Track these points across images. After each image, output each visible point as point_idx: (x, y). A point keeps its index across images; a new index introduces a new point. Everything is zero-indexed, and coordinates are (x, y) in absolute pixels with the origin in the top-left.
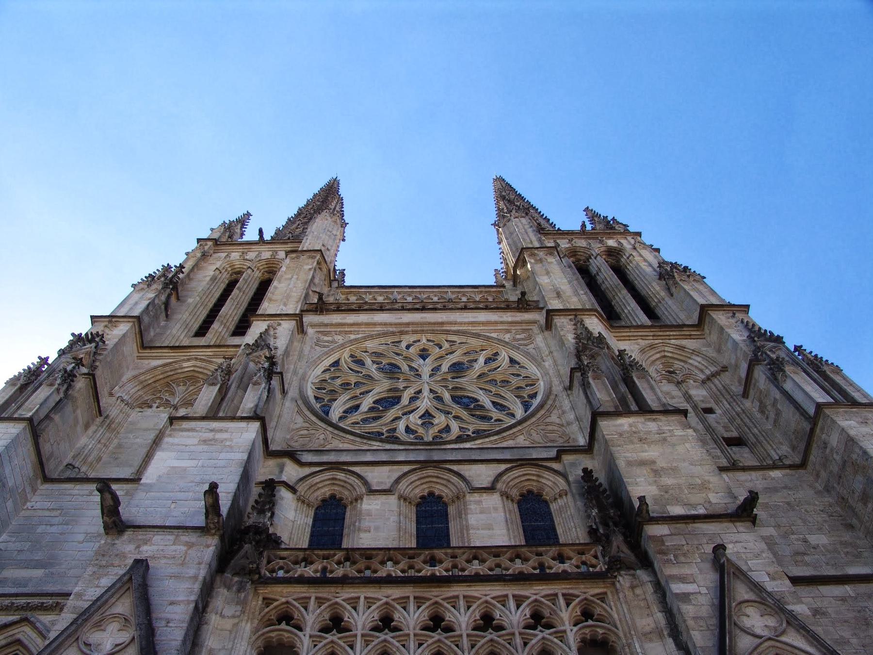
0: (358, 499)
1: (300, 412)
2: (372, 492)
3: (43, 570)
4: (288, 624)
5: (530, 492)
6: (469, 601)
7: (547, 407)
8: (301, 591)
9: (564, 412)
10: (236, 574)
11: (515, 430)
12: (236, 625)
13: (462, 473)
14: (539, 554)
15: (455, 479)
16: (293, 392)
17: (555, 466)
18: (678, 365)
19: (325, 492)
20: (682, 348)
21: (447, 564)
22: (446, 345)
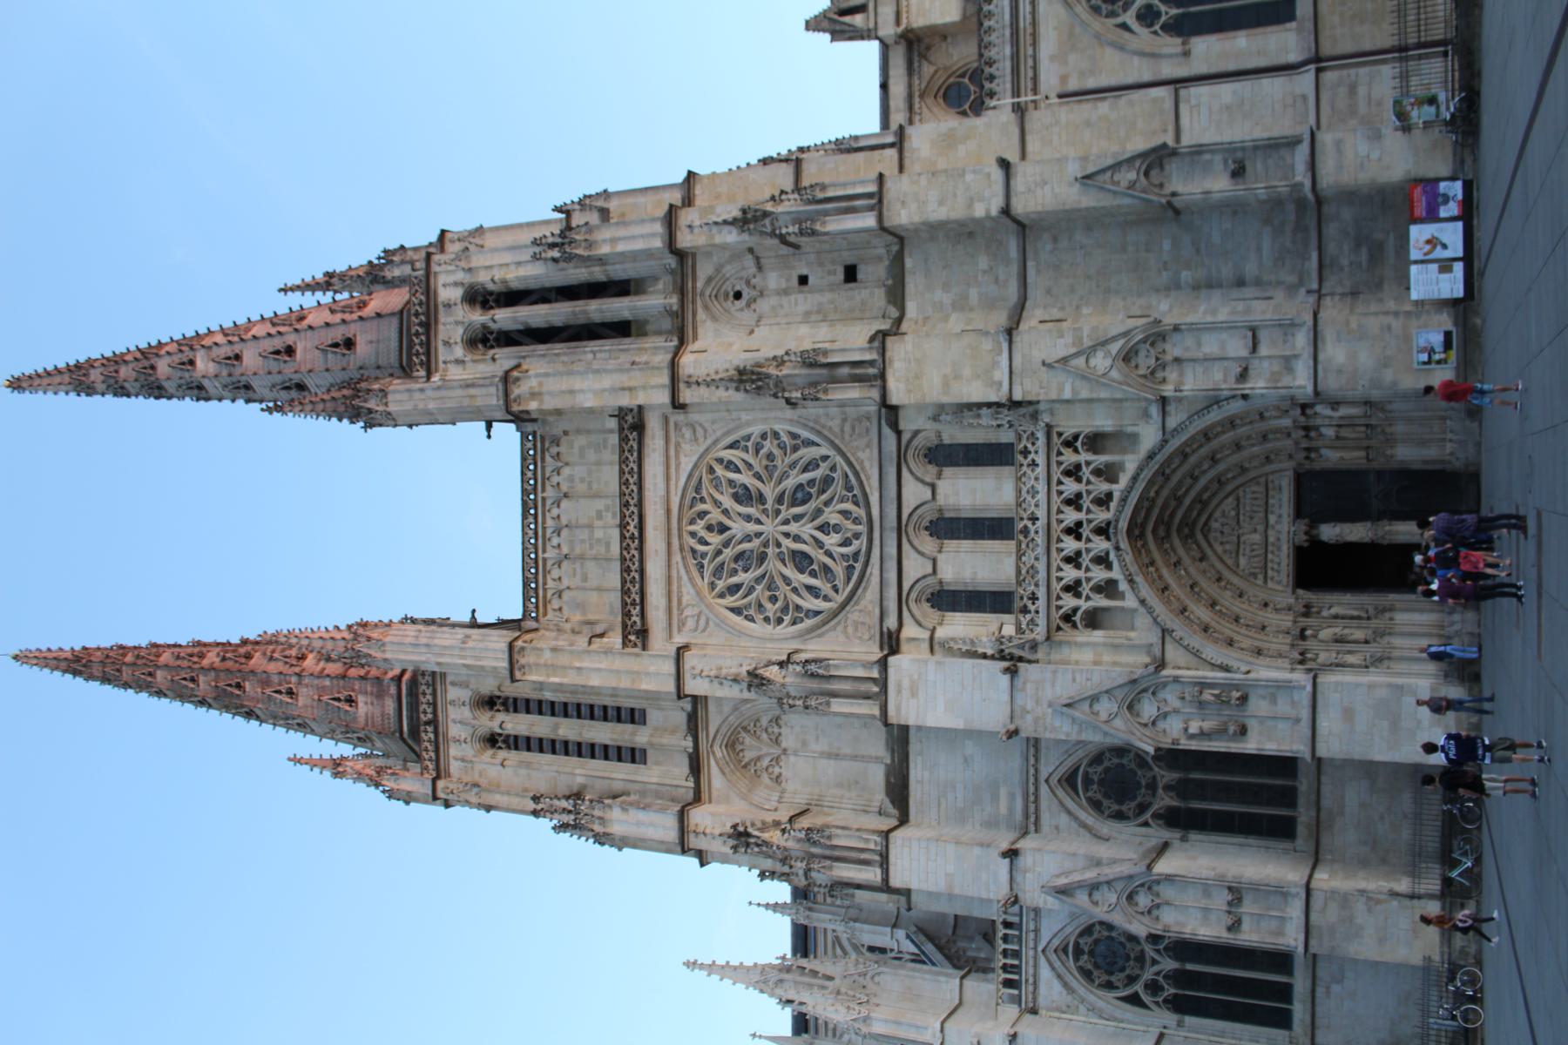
0: (941, 582)
1: (820, 636)
2: (935, 571)
5: (925, 456)
6: (1060, 511)
7: (818, 428)
9: (827, 415)
11: (852, 459)
14: (1022, 465)
15: (919, 512)
16: (795, 645)
17: (906, 437)
18: (728, 287)
19: (926, 606)
20: (709, 280)
21: (1029, 524)
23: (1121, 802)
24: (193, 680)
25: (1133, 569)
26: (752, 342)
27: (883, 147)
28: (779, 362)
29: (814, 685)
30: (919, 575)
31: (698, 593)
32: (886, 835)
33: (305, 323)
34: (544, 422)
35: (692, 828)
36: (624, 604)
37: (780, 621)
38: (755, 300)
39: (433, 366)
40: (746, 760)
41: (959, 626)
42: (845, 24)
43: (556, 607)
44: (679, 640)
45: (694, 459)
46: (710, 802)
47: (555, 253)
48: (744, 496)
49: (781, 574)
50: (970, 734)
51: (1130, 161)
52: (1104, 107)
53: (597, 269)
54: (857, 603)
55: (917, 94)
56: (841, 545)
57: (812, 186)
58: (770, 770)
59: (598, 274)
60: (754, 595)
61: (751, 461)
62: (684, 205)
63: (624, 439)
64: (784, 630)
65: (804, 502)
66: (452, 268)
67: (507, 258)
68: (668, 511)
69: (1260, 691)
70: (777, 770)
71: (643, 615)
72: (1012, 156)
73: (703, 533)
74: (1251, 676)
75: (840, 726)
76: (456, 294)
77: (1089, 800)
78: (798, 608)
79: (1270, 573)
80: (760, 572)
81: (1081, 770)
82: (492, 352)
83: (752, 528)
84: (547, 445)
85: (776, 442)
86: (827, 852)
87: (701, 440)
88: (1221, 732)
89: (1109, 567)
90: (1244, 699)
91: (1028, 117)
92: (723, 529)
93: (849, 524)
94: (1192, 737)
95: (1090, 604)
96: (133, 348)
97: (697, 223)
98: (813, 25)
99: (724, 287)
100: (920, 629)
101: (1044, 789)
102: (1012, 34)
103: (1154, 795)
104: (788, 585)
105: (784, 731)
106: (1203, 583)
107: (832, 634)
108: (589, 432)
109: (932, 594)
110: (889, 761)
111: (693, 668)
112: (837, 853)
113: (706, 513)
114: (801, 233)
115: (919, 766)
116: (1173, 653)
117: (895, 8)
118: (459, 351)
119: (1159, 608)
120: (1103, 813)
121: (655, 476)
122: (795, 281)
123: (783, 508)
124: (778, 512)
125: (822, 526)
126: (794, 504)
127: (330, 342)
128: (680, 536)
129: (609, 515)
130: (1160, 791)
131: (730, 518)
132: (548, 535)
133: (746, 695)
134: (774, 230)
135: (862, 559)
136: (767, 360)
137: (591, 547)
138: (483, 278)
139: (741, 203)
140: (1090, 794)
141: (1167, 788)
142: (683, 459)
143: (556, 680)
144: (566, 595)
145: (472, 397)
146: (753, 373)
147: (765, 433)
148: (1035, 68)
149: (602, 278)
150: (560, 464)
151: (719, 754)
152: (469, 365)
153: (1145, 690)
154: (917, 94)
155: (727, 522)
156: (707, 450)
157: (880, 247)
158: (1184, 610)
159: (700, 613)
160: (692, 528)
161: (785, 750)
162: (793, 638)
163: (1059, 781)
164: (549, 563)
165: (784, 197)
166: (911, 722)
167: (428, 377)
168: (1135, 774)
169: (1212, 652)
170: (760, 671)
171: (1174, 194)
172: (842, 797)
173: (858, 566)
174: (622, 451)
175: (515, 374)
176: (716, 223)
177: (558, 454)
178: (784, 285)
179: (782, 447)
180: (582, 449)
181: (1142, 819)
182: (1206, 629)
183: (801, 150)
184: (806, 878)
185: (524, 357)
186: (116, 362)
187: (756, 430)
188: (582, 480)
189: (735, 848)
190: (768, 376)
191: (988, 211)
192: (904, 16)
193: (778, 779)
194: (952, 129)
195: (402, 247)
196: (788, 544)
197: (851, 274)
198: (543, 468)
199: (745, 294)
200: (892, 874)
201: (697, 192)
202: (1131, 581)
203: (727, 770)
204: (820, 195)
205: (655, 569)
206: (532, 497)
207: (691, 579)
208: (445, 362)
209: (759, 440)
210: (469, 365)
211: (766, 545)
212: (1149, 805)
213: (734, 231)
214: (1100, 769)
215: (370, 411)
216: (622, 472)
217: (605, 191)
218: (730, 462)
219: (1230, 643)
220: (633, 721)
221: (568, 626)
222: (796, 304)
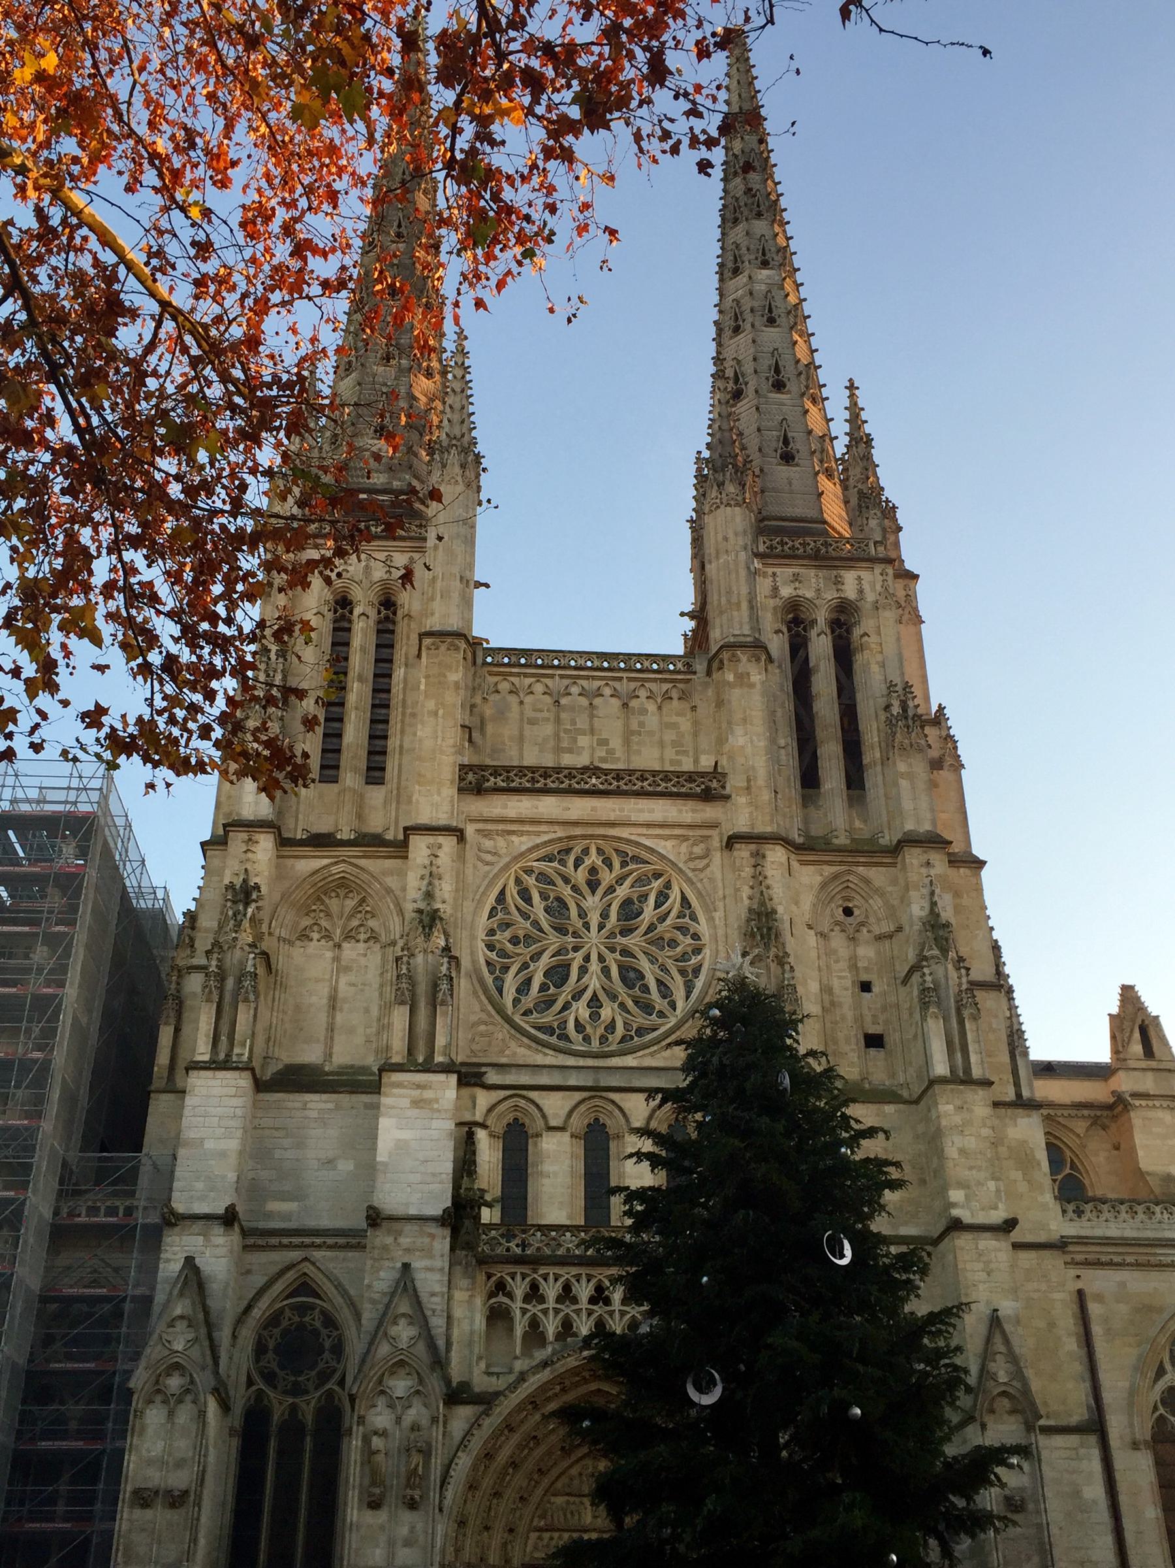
0: (538, 1135)
1: (475, 993)
3: (296, 1204)
4: (504, 1295)
8: (511, 1268)
10: (463, 1249)
12: (471, 1296)
13: (622, 1104)
15: (617, 1112)
16: (465, 963)
18: (855, 903)
19: (510, 1118)
20: (867, 881)
22: (616, 864)
23: (276, 1351)
24: (399, 235)
25: (560, 1367)
26: (800, 928)
27: (1017, 1084)
28: (781, 960)
29: (422, 988)
30: (545, 1109)
31: (522, 855)
32: (248, 1068)
33: (808, 404)
34: (706, 685)
35: (257, 837)
36: (508, 769)
37: (490, 947)
38: (843, 931)
39: (770, 561)
40: (327, 901)
41: (489, 1154)
42: (1132, 1031)
43: (500, 687)
44: (470, 830)
45: (672, 857)
46: (278, 857)
47: (896, 709)
48: (630, 910)
49: (544, 951)
50: (369, 1169)
51: (1018, 1374)
52: (1071, 1344)
53: (878, 755)
54: (512, 1037)
55: (1052, 1112)
56: (576, 1020)
57: (976, 1004)
58: (316, 928)
59: (871, 754)
60: (520, 919)
61: (668, 922)
62: (949, 854)
63: (691, 777)
64: (482, 953)
65: (623, 979)
66: (878, 588)
67: (890, 649)
68: (612, 824)
69: (419, 1527)
70: (315, 936)
71: (497, 790)
72: (1016, 1235)
73: (588, 862)
74: (438, 1516)
75: (367, 1010)
76: (850, 592)
77: (281, 1311)
78: (506, 969)
79: (546, 1535)
80: (545, 925)
81: (318, 1301)
82: (785, 630)
83: (594, 919)
84: (680, 686)
85: (689, 950)
86: (228, 997)
87: (692, 865)
88: (375, 1477)
89: (559, 1337)
90: (412, 1505)
91: (1055, 1253)
92: (593, 885)
93: (601, 1030)
94: (366, 1440)
95: (518, 1313)
96: (780, 189)
97: (933, 872)
98: (1128, 994)
99: (858, 897)
100: (485, 1111)
101: (296, 1255)
102: (1148, 1239)
103: (285, 1392)
104: (532, 958)
105: (361, 945)
106: (539, 1452)
107: (477, 1008)
108: (695, 735)
109: (523, 1125)
110: (327, 1069)
111: (440, 846)
112: (227, 1007)
113: (611, 869)
114: (924, 991)
115: (323, 1106)
116: (463, 1414)
117: (1152, 1093)
118: (786, 592)
119: (515, 1398)
120: (265, 1328)
121: (651, 811)
122: (865, 977)
123: (617, 956)
124: (612, 950)
125: (598, 1000)
126: (621, 967)
127: (790, 435)
128: (584, 837)
129: (603, 754)
130: (291, 1400)
131: (605, 894)
132: (580, 682)
133: (409, 907)
134: (926, 958)
135: (562, 1044)
136: (783, 944)
137: (566, 731)
138: (866, 624)
139: (953, 921)
140: (287, 1310)
141: (294, 1408)
142: (669, 844)
143: (422, 687)
144: (513, 699)
145: (738, 604)
146: (769, 929)
147: (699, 939)
148: (1111, 1264)
149: (866, 760)
150: (659, 700)
151: (334, 869)
152: (772, 603)
153: (421, 1381)
154: (1052, 1112)
155: (600, 891)
156: (680, 870)
157: (906, 1078)
158: (511, 1430)
159: (499, 856)
160: (593, 851)
161: (339, 946)
162: (474, 962)
163: (305, 1274)
164: (548, 681)
165: (963, 971)
166: (385, 1100)
167: (757, 555)
168: (312, 1368)
169: (464, 1462)
170: (439, 926)
171: (983, 1426)
172: (284, 1012)
173: (553, 1040)
174: (679, 775)
175: (763, 658)
176: (932, 893)
177: (671, 698)
178: (860, 964)
179: (684, 957)
180: (675, 726)
181: (256, 1377)
182: (489, 1456)
183: (1010, 990)
184: (188, 968)
185: (780, 667)
186: (765, 169)
187: (703, 928)
188: (642, 724)
189: (231, 887)
190: (767, 946)
191: (954, 1205)
192: (1143, 1103)
193: (304, 936)
194: (1039, 1164)
195: (900, 529)
196: (578, 959)
197: (874, 1041)
198: (655, 680)
199: (850, 919)
200: (203, 1073)
201: (962, 870)
202: (545, 1364)
203: (317, 877)
204: (966, 1013)
205: (548, 806)
206: (622, 665)
207: (536, 847)
208: (774, 574)
209: (692, 931)
210: (772, 603)
211: (575, 934)
212: (275, 1388)
213: (923, 914)
214: (318, 1324)
215: (721, 485)
216: (654, 773)
217: (963, 766)
218: (667, 897)
219: (472, 1487)
220: (369, 769)
221: (478, 700)
222: (840, 978)
